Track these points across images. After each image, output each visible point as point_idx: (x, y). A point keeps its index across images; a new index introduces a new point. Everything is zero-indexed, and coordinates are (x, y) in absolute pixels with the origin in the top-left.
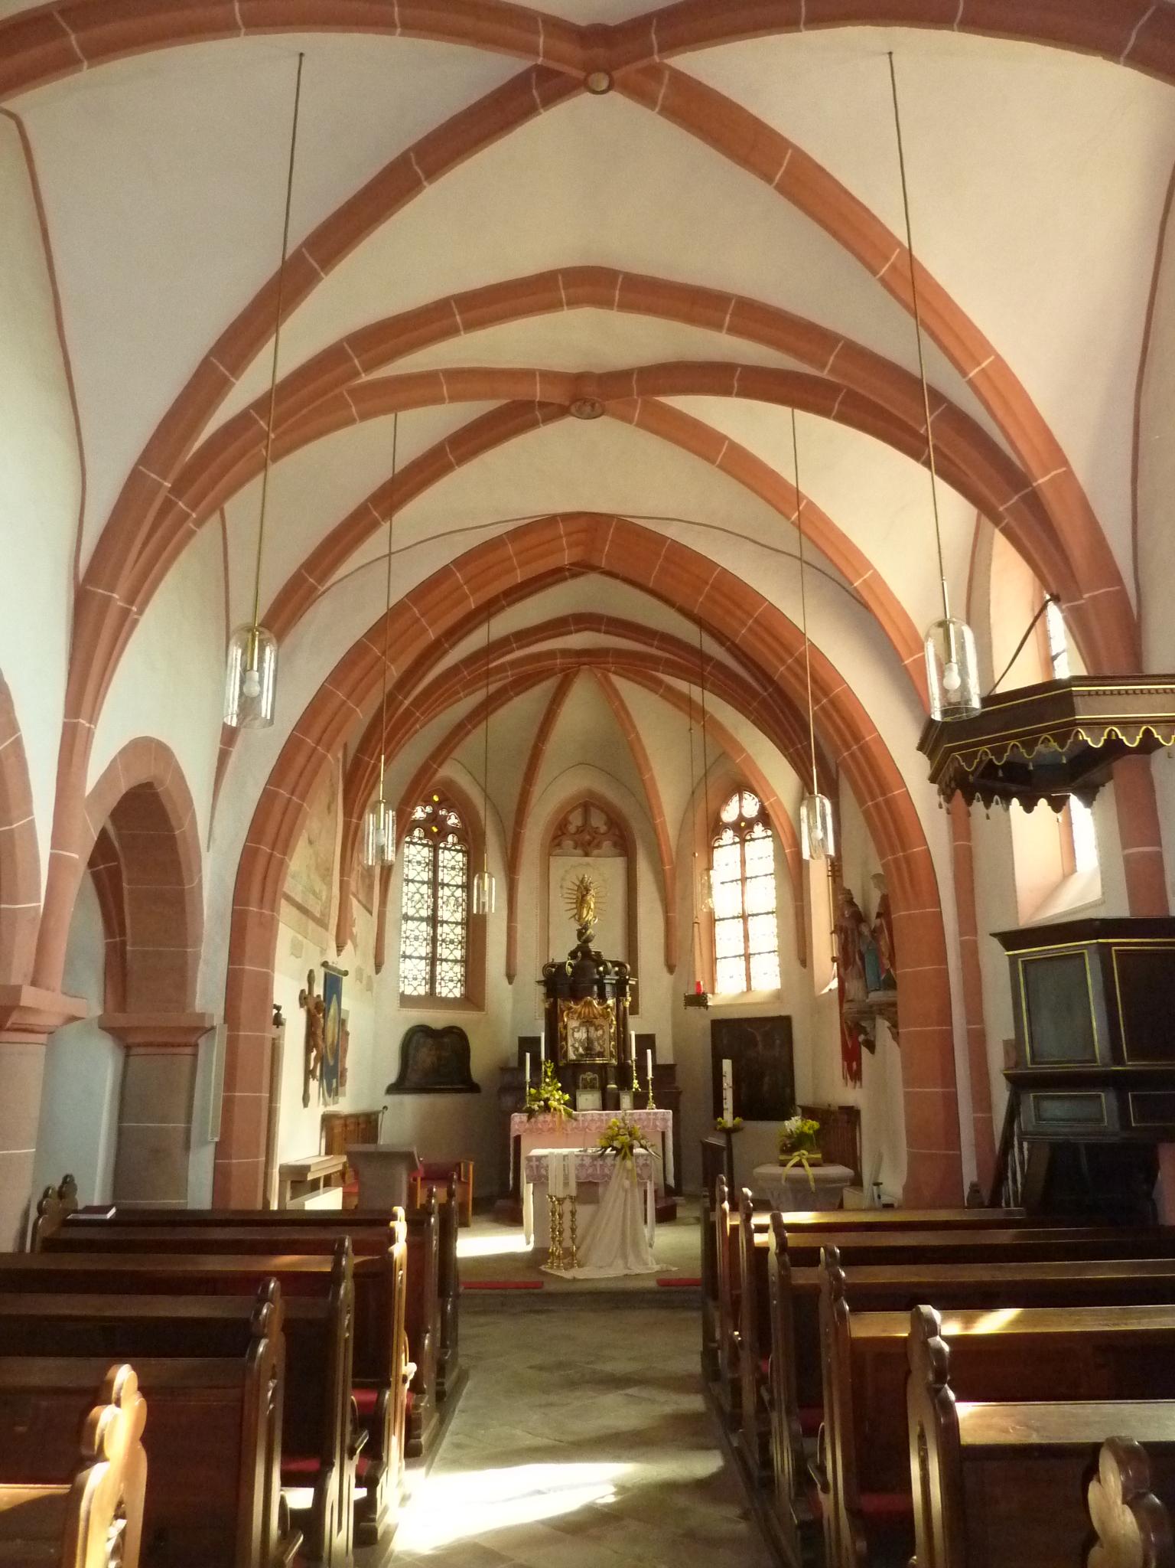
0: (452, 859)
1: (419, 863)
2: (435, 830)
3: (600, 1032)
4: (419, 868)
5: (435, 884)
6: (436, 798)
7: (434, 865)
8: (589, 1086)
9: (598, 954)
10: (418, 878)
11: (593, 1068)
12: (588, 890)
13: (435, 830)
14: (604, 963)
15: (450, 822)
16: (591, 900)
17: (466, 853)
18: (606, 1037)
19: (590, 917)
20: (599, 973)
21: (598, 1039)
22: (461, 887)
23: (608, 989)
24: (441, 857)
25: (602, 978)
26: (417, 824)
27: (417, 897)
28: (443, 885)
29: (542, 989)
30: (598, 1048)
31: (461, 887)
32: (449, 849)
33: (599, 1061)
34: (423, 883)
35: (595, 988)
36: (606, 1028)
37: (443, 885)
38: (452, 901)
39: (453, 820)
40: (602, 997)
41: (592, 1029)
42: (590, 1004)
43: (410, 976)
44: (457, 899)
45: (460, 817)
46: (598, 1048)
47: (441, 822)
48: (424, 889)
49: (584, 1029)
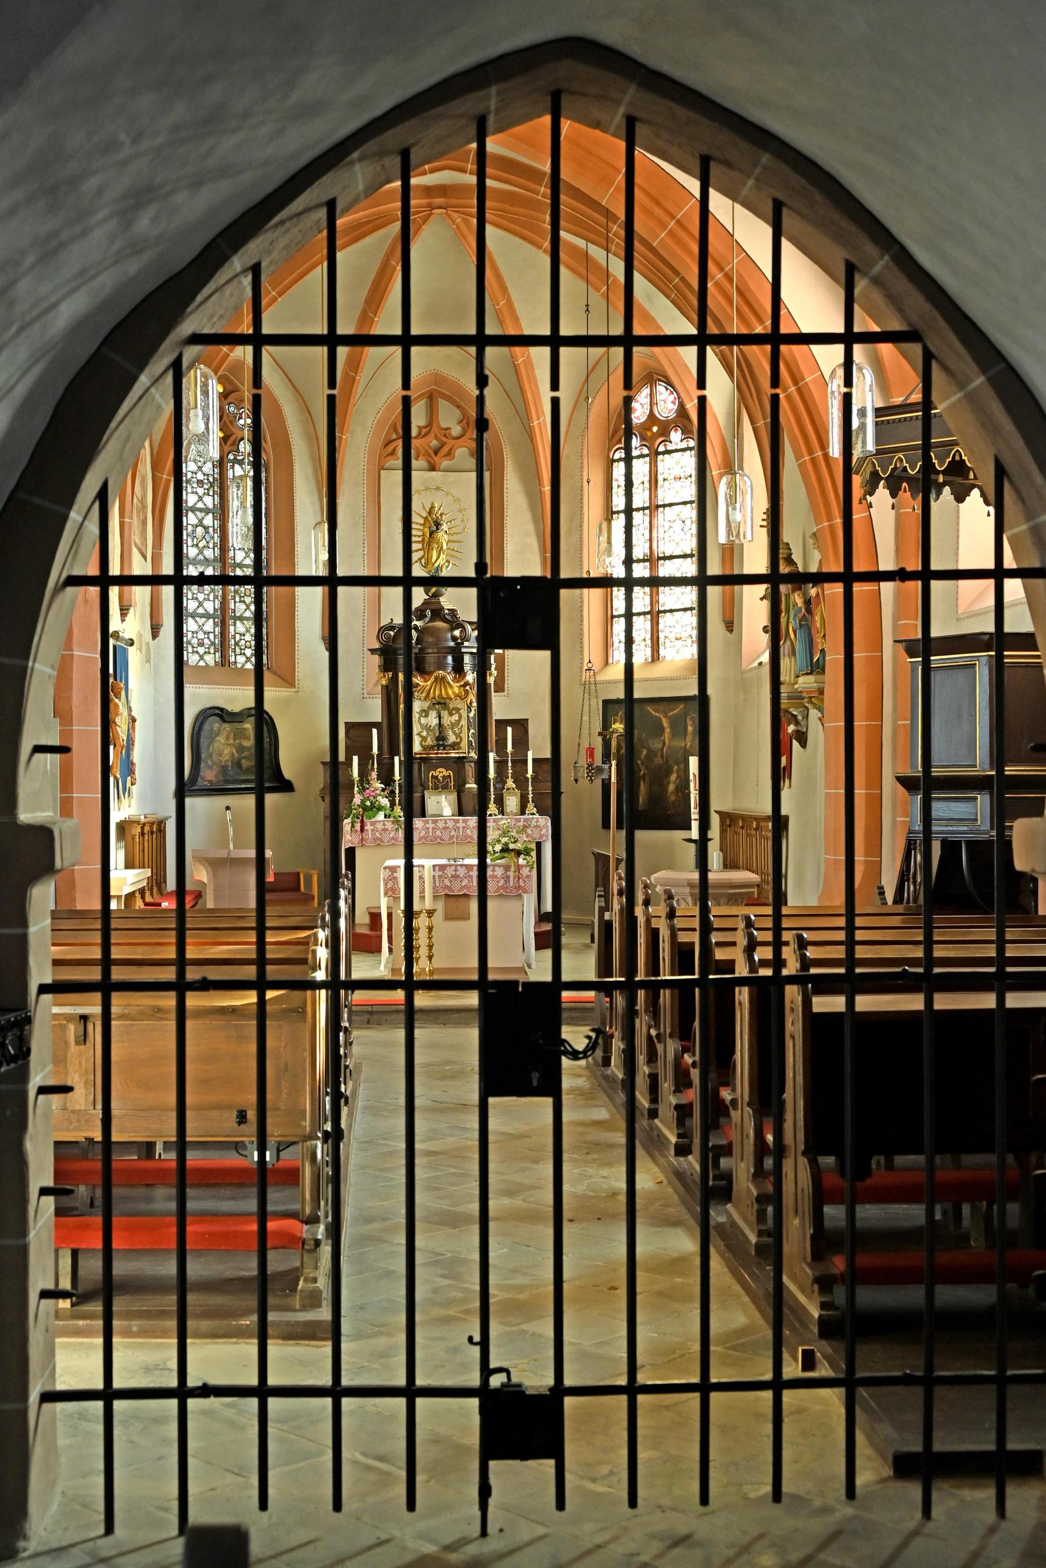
1: (200, 483)
3: (456, 717)
4: (201, 491)
8: (441, 786)
9: (453, 612)
10: (200, 505)
11: (445, 762)
12: (438, 525)
14: (460, 625)
16: (442, 537)
18: (464, 722)
19: (441, 561)
20: (454, 639)
21: (453, 725)
23: (467, 659)
25: (459, 645)
27: (200, 531)
29: (376, 660)
30: (452, 739)
33: (453, 754)
34: (207, 511)
35: (450, 659)
36: (464, 712)
40: (459, 669)
41: (445, 714)
42: (442, 680)
43: (195, 641)
46: (452, 739)
48: (208, 520)
49: (433, 714)
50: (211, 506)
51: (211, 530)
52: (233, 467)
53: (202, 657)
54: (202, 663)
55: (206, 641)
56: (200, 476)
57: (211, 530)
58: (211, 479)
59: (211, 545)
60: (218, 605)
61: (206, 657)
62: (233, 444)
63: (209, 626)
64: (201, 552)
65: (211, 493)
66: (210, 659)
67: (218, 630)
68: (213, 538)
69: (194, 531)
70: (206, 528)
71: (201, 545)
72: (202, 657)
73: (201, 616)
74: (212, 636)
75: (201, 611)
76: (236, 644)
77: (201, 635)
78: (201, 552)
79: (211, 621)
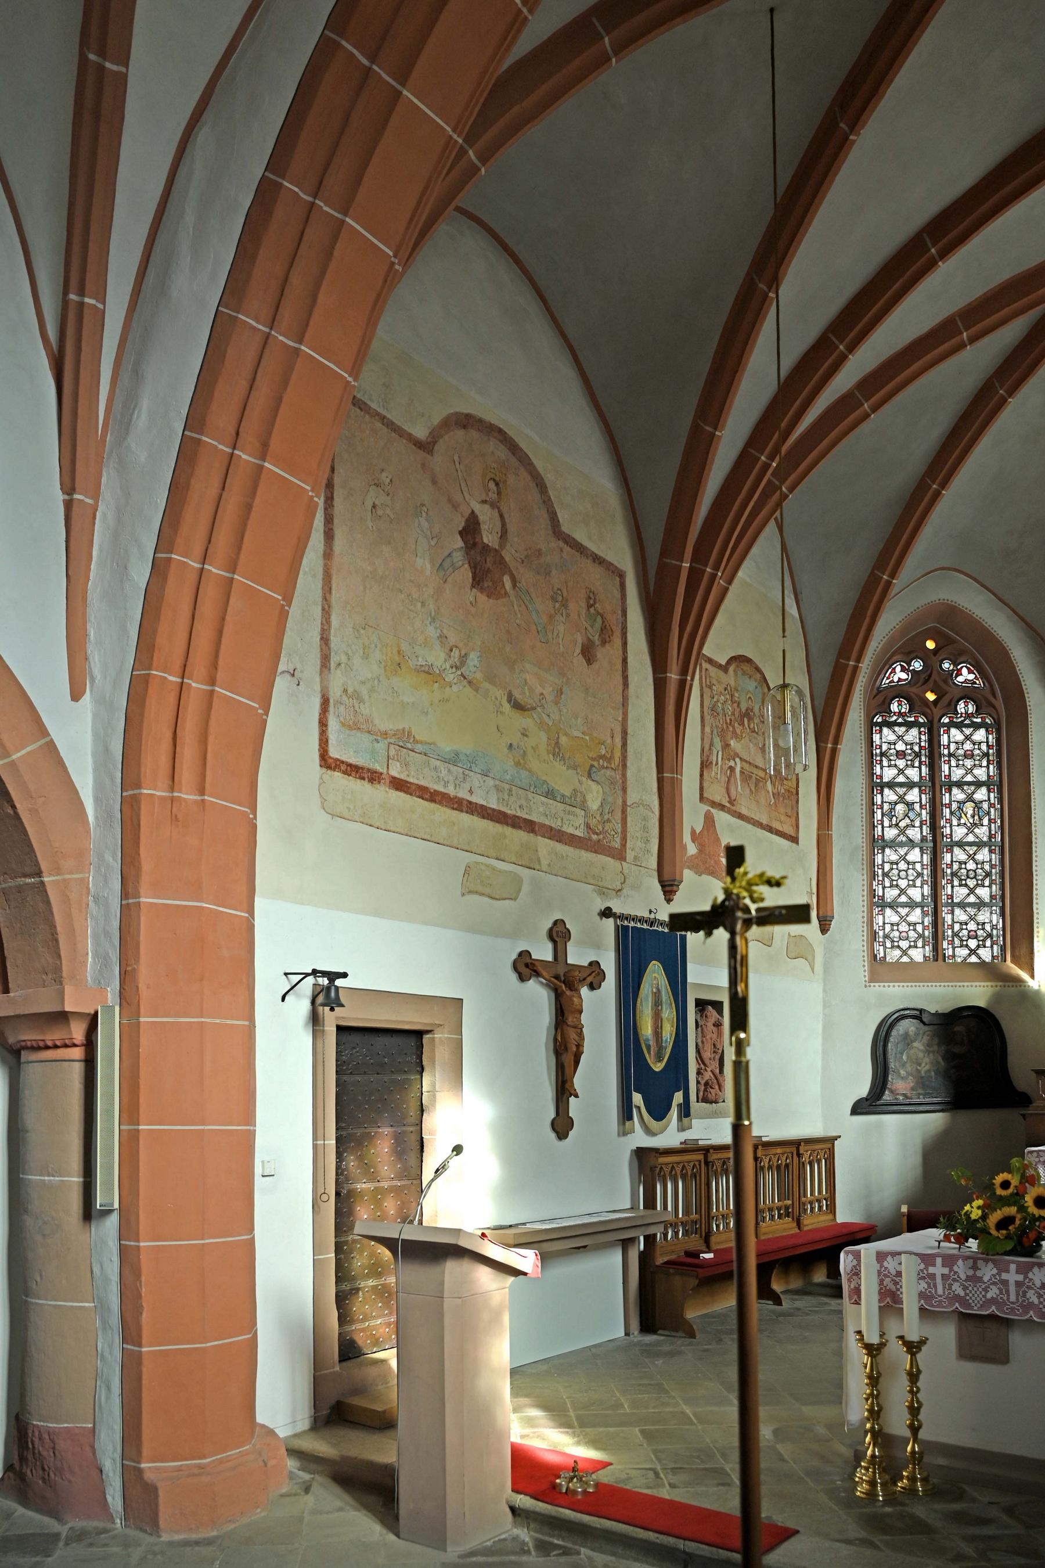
0: (968, 744)
1: (901, 755)
2: (931, 697)
5: (935, 785)
6: (930, 645)
7: (933, 754)
10: (901, 779)
13: (931, 697)
15: (960, 679)
17: (996, 727)
22: (988, 784)
24: (944, 740)
26: (898, 692)
28: (950, 785)
31: (988, 784)
32: (959, 726)
37: (950, 785)
38: (969, 808)
39: (966, 675)
44: (978, 805)
45: (977, 667)
47: (943, 684)
50: (916, 779)
51: (917, 807)
52: (948, 732)
53: (905, 953)
54: (905, 959)
55: (912, 934)
56: (901, 747)
57: (917, 807)
58: (916, 748)
59: (917, 824)
60: (927, 890)
61: (911, 952)
62: (949, 704)
63: (916, 915)
64: (902, 832)
65: (917, 764)
66: (917, 955)
67: (927, 921)
68: (920, 815)
69: (892, 809)
70: (910, 805)
71: (902, 824)
72: (905, 953)
73: (904, 905)
74: (919, 928)
75: (903, 899)
76: (955, 935)
77: (904, 927)
78: (902, 832)
79: (918, 911)
